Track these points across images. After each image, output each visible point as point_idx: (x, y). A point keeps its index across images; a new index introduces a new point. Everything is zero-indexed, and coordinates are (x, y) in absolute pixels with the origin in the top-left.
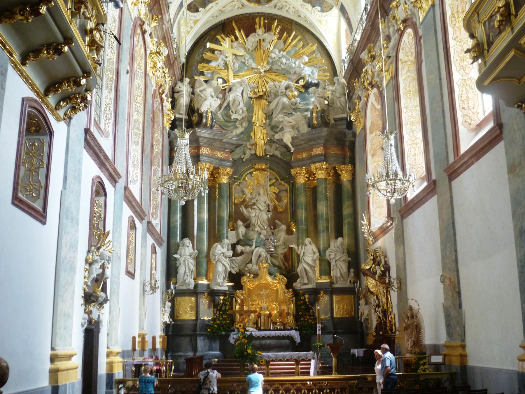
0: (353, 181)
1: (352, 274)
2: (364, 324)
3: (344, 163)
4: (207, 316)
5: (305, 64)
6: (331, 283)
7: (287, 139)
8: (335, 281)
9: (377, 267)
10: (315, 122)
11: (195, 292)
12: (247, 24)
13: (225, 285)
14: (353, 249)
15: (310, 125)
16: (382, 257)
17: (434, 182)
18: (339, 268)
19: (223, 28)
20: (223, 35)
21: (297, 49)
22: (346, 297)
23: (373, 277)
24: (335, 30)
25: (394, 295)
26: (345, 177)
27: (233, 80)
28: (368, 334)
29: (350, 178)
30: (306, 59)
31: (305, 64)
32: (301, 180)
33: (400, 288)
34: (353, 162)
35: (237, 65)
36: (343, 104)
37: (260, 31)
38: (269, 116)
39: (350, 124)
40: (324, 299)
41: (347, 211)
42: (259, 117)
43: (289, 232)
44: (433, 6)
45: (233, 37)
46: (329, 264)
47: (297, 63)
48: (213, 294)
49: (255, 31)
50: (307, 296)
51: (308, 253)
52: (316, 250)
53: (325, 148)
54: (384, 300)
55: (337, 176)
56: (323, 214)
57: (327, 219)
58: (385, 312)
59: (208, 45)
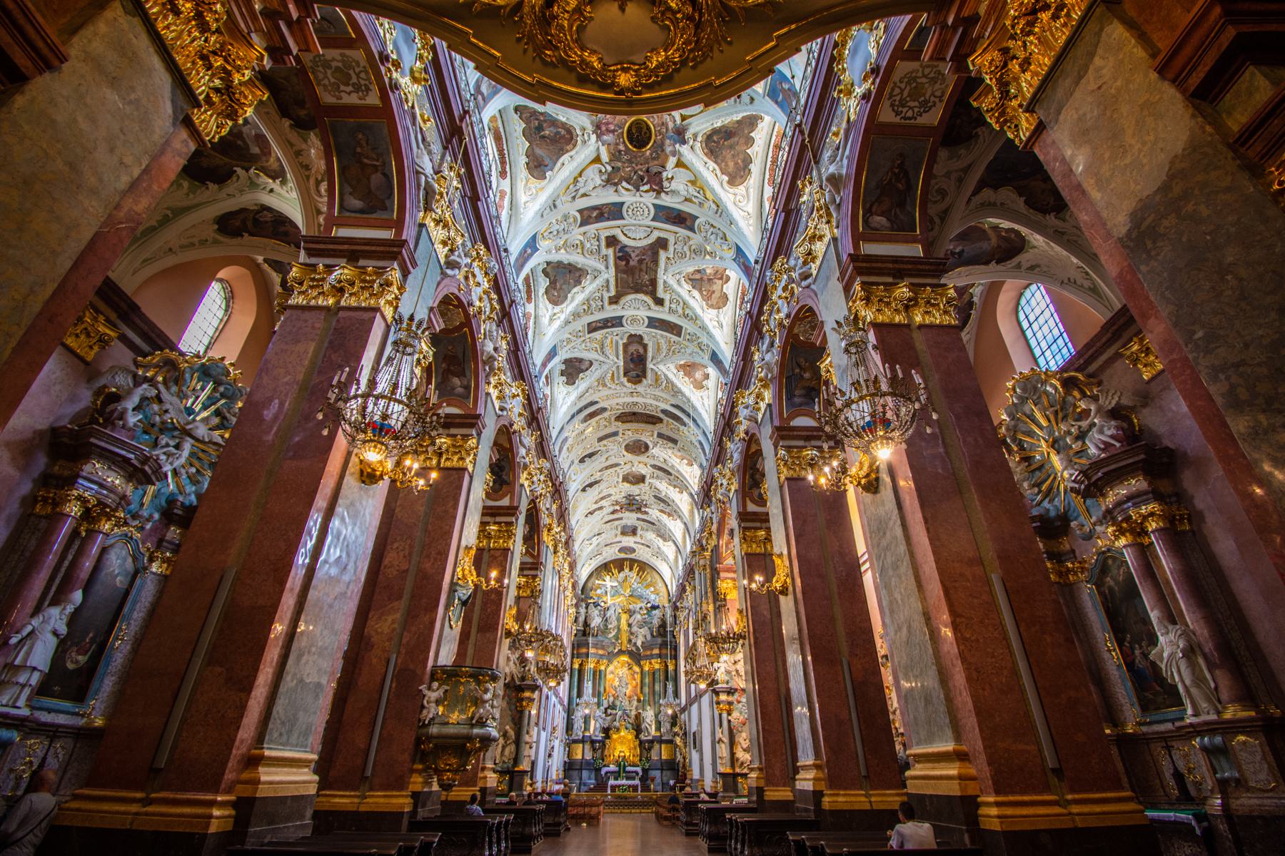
4: (588, 756)
7: (639, 644)
11: (583, 741)
12: (619, 564)
13: (600, 736)
18: (666, 727)
19: (605, 567)
26: (671, 668)
27: (610, 602)
32: (646, 668)
37: (627, 570)
38: (630, 625)
40: (657, 746)
42: (624, 626)
43: (639, 701)
48: (593, 742)
51: (649, 715)
55: (667, 666)
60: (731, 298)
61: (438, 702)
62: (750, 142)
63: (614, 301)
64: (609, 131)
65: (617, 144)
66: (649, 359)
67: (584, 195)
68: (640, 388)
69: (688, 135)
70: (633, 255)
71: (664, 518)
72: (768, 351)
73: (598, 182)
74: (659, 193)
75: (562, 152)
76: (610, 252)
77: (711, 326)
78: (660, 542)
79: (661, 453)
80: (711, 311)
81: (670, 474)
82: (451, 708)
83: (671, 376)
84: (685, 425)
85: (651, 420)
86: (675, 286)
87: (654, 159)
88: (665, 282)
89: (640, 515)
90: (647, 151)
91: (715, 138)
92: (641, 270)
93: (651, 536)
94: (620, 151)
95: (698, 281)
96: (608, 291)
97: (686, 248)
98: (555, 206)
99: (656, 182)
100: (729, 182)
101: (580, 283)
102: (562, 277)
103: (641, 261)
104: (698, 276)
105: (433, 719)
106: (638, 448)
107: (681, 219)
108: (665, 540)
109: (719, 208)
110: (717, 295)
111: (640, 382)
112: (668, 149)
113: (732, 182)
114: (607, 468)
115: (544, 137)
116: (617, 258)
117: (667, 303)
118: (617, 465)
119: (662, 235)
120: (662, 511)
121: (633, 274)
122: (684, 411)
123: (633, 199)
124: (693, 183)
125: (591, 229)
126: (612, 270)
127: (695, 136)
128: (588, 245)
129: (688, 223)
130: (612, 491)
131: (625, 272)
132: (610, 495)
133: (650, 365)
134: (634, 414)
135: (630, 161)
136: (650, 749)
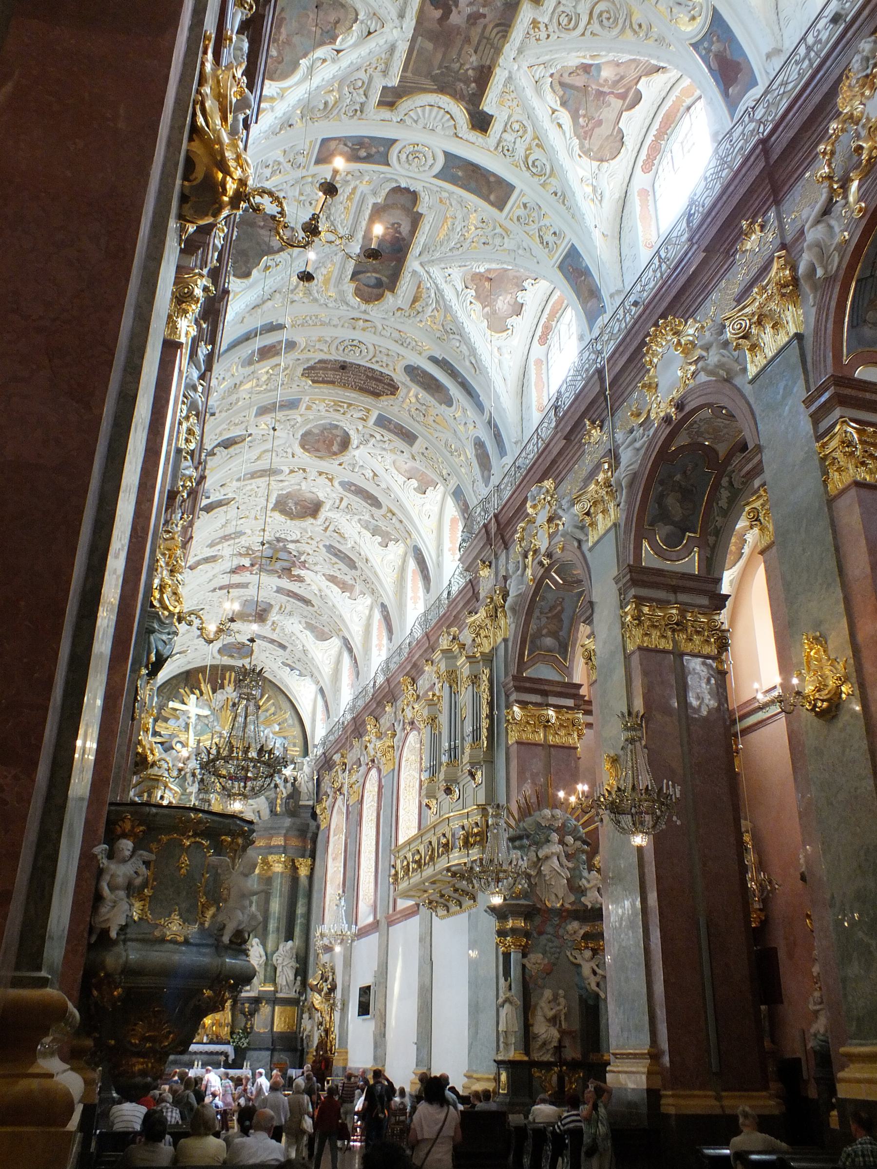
0: (311, 877)
1: (298, 983)
2: (305, 1042)
3: (303, 856)
5: (274, 733)
6: (276, 991)
8: (279, 990)
9: (324, 984)
10: (278, 809)
14: (302, 954)
15: (273, 812)
16: (330, 974)
17: (378, 922)
18: (286, 975)
20: (186, 689)
21: (268, 714)
22: (289, 1008)
23: (320, 994)
24: (312, 696)
25: (337, 1016)
26: (303, 872)
28: (308, 1053)
29: (308, 873)
30: (277, 728)
31: (274, 733)
33: (342, 1010)
34: (313, 856)
35: (199, 727)
36: (311, 790)
39: (314, 816)
40: (265, 1009)
41: (300, 910)
44: (393, 770)
45: (197, 692)
46: (275, 969)
47: (266, 732)
49: (222, 687)
50: (247, 1005)
52: (263, 953)
53: (285, 840)
54: (328, 1019)
55: (295, 869)
56: (275, 913)
57: (279, 918)
58: (327, 1031)
59: (171, 704)
60: (631, 143)
61: (132, 890)
63: (391, 99)
66: (415, 249)
68: (375, 312)
71: (334, 593)
77: (581, 193)
78: (308, 639)
79: (375, 460)
81: (375, 503)
82: (159, 903)
83: (449, 294)
84: (449, 402)
85: (377, 385)
86: (530, 93)
89: (285, 583)
92: (467, 40)
93: (291, 625)
96: (385, 73)
101: (333, 39)
103: (473, 19)
104: (579, 81)
105: (123, 929)
106: (330, 443)
108: (322, 636)
110: (604, 130)
111: (379, 297)
114: (253, 475)
117: (496, 128)
118: (270, 472)
120: (332, 579)
122: (453, 373)
126: (410, 23)
130: (246, 526)
132: (240, 534)
133: (412, 263)
134: (343, 367)
136: (252, 1014)
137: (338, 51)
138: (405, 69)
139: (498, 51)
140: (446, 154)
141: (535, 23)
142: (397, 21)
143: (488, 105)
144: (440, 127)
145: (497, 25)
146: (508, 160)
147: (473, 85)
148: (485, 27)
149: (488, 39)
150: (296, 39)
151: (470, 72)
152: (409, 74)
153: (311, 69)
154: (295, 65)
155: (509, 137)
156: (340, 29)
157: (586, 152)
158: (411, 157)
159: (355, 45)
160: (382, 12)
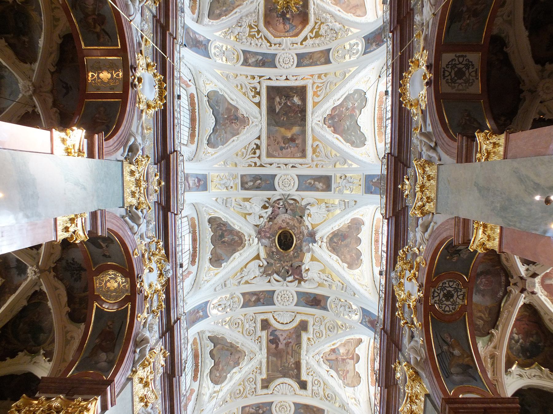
62: (359, 241)
63: (266, 384)
64: (266, 237)
65: (271, 247)
67: (247, 282)
69: (317, 237)
70: (281, 338)
72: (410, 342)
73: (257, 273)
74: (299, 283)
75: (234, 251)
76: (264, 334)
80: (347, 388)
86: (316, 366)
87: (295, 257)
88: (307, 363)
90: (291, 251)
91: (335, 240)
92: (288, 353)
94: (273, 252)
95: (335, 361)
96: (260, 373)
97: (322, 328)
98: (225, 285)
99: (296, 272)
100: (348, 267)
101: (239, 364)
102: (225, 354)
103: (287, 344)
107: (316, 301)
109: (345, 287)
112: (305, 249)
113: (350, 266)
115: (224, 242)
116: (271, 341)
117: (309, 386)
119: (304, 318)
121: (281, 357)
123: (282, 288)
124: (323, 271)
125: (251, 310)
126: (265, 351)
127: (322, 238)
128: (247, 326)
129: (322, 304)
131: (275, 355)
135: (279, 260)
137: (241, 368)
138: (268, 370)
139: (300, 354)
140: (295, 404)
141: (309, 339)
142: (259, 352)
143: (304, 377)
144: (288, 392)
145: (296, 345)
146: (319, 398)
147: (295, 370)
148: (292, 346)
149: (295, 351)
150: (225, 368)
151: (293, 366)
152: (270, 372)
153: (231, 378)
154: (226, 377)
155: (315, 388)
156: (241, 360)
157: (348, 385)
158: (280, 409)
159: (246, 365)
160: (253, 350)
